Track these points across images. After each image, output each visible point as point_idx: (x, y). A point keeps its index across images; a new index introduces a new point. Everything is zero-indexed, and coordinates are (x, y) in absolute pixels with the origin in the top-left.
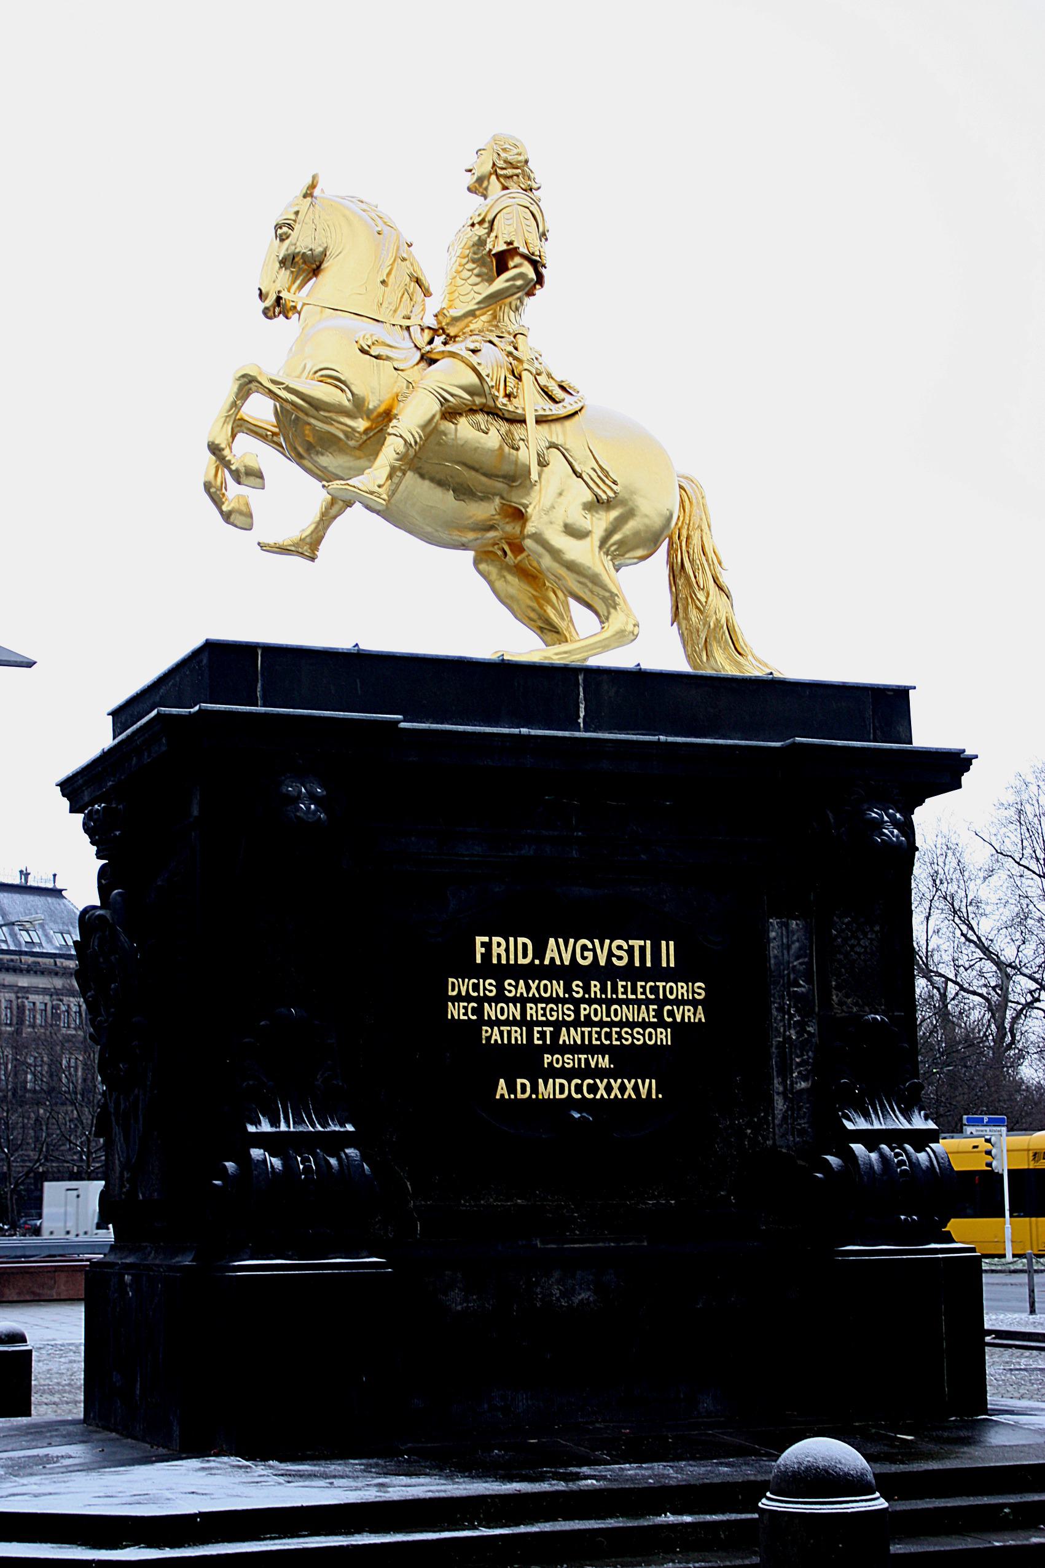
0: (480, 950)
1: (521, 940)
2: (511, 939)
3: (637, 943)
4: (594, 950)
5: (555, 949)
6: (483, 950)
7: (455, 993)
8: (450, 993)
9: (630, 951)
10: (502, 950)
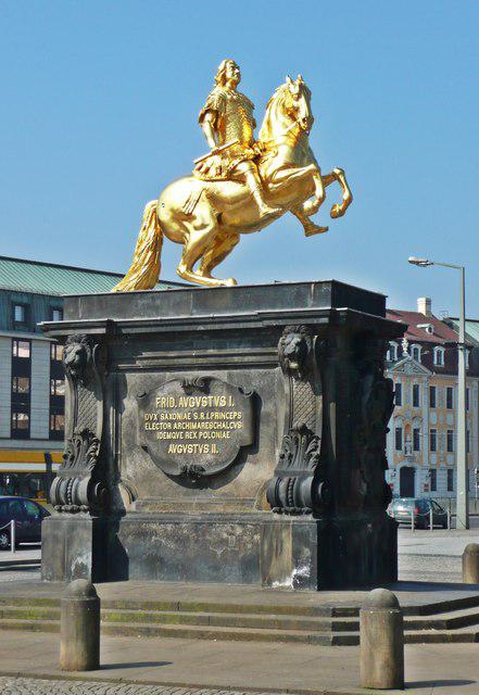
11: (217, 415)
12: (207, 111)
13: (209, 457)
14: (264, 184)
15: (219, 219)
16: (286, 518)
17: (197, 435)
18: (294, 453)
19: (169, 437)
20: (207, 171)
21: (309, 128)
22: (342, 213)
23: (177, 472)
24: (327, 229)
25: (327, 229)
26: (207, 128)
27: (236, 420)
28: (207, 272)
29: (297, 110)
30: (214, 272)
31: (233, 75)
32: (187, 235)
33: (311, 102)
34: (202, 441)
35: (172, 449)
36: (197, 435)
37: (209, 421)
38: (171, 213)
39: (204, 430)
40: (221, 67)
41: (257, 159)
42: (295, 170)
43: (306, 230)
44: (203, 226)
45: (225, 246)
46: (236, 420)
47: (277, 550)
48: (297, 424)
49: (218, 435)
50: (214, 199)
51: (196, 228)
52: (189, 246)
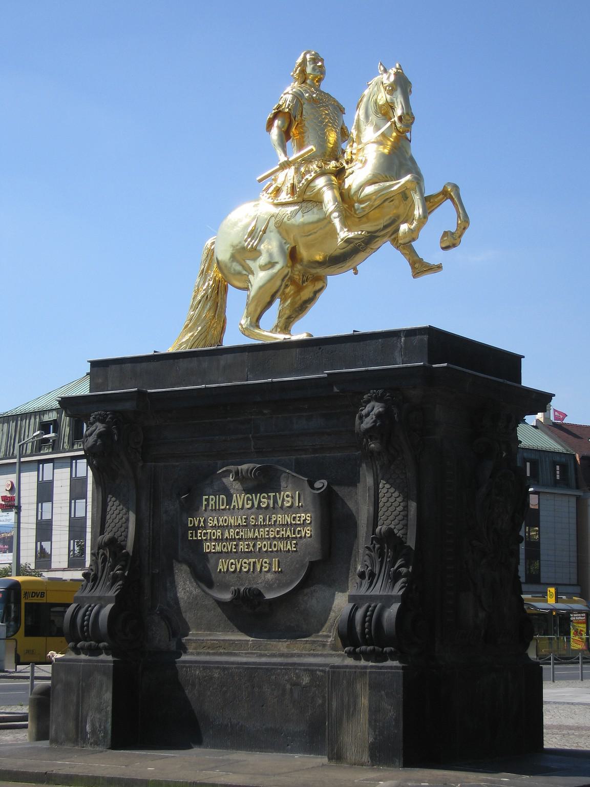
0: (205, 503)
1: (221, 496)
2: (217, 496)
3: (272, 494)
4: (252, 500)
5: (236, 502)
6: (206, 503)
7: (192, 525)
8: (189, 525)
9: (269, 498)
10: (213, 502)
11: (280, 518)
12: (276, 116)
13: (269, 576)
16: (363, 663)
17: (254, 546)
18: (377, 570)
19: (218, 549)
20: (278, 191)
23: (227, 596)
24: (439, 267)
25: (439, 267)
26: (275, 132)
27: (304, 524)
28: (286, 327)
29: (391, 106)
30: (295, 327)
31: (314, 69)
32: (251, 277)
33: (411, 98)
34: (260, 554)
35: (222, 566)
36: (254, 546)
37: (270, 526)
39: (262, 539)
40: (299, 60)
41: (340, 173)
43: (413, 267)
45: (306, 294)
46: (304, 524)
47: (350, 709)
48: (381, 528)
49: (281, 545)
52: (253, 291)
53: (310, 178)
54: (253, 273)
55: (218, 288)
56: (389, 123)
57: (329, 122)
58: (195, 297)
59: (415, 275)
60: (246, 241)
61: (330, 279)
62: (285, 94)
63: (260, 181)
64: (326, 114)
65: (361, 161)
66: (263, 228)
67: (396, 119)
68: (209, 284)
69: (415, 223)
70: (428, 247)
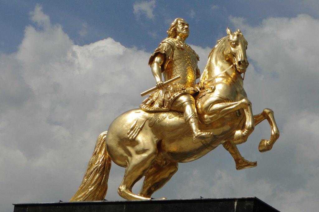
12: (156, 55)
14: (199, 116)
15: (159, 146)
20: (152, 104)
21: (244, 71)
22: (269, 147)
24: (255, 164)
25: (255, 164)
32: (129, 158)
38: (118, 140)
42: (229, 104)
44: (144, 151)
50: (156, 128)
51: (138, 153)
52: (130, 167)
53: (176, 96)
54: (130, 155)
55: (105, 165)
56: (232, 66)
57: (190, 63)
58: (89, 169)
59: (237, 169)
60: (128, 134)
61: (180, 165)
62: (162, 43)
63: (142, 95)
64: (188, 58)
65: (212, 88)
66: (141, 127)
67: (237, 63)
68: (99, 161)
69: (246, 131)
70: (247, 151)
